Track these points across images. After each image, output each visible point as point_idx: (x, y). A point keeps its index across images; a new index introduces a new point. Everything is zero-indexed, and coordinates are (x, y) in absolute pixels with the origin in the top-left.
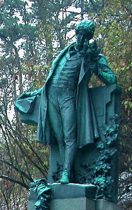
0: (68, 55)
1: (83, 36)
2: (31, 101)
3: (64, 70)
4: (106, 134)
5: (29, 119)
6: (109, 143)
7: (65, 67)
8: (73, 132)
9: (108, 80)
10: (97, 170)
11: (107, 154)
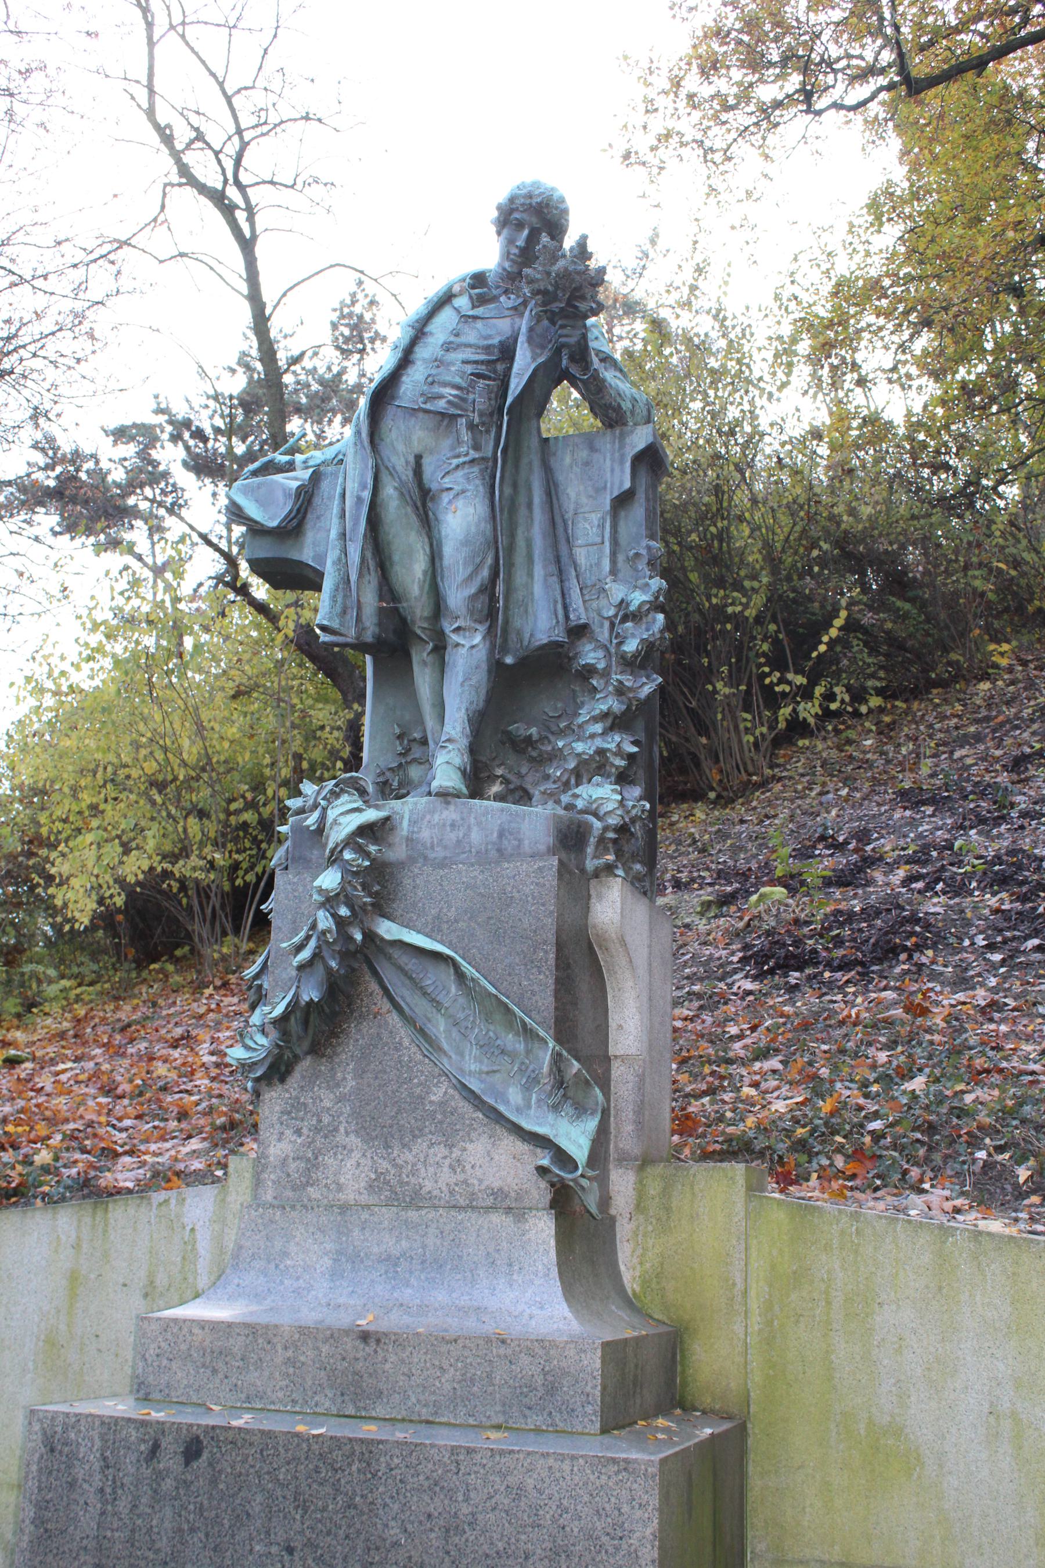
0: (462, 302)
1: (526, 232)
2: (295, 484)
3: (448, 347)
4: (616, 616)
5: (284, 555)
6: (631, 646)
7: (452, 339)
8: (482, 590)
9: (623, 404)
10: (579, 755)
11: (620, 691)
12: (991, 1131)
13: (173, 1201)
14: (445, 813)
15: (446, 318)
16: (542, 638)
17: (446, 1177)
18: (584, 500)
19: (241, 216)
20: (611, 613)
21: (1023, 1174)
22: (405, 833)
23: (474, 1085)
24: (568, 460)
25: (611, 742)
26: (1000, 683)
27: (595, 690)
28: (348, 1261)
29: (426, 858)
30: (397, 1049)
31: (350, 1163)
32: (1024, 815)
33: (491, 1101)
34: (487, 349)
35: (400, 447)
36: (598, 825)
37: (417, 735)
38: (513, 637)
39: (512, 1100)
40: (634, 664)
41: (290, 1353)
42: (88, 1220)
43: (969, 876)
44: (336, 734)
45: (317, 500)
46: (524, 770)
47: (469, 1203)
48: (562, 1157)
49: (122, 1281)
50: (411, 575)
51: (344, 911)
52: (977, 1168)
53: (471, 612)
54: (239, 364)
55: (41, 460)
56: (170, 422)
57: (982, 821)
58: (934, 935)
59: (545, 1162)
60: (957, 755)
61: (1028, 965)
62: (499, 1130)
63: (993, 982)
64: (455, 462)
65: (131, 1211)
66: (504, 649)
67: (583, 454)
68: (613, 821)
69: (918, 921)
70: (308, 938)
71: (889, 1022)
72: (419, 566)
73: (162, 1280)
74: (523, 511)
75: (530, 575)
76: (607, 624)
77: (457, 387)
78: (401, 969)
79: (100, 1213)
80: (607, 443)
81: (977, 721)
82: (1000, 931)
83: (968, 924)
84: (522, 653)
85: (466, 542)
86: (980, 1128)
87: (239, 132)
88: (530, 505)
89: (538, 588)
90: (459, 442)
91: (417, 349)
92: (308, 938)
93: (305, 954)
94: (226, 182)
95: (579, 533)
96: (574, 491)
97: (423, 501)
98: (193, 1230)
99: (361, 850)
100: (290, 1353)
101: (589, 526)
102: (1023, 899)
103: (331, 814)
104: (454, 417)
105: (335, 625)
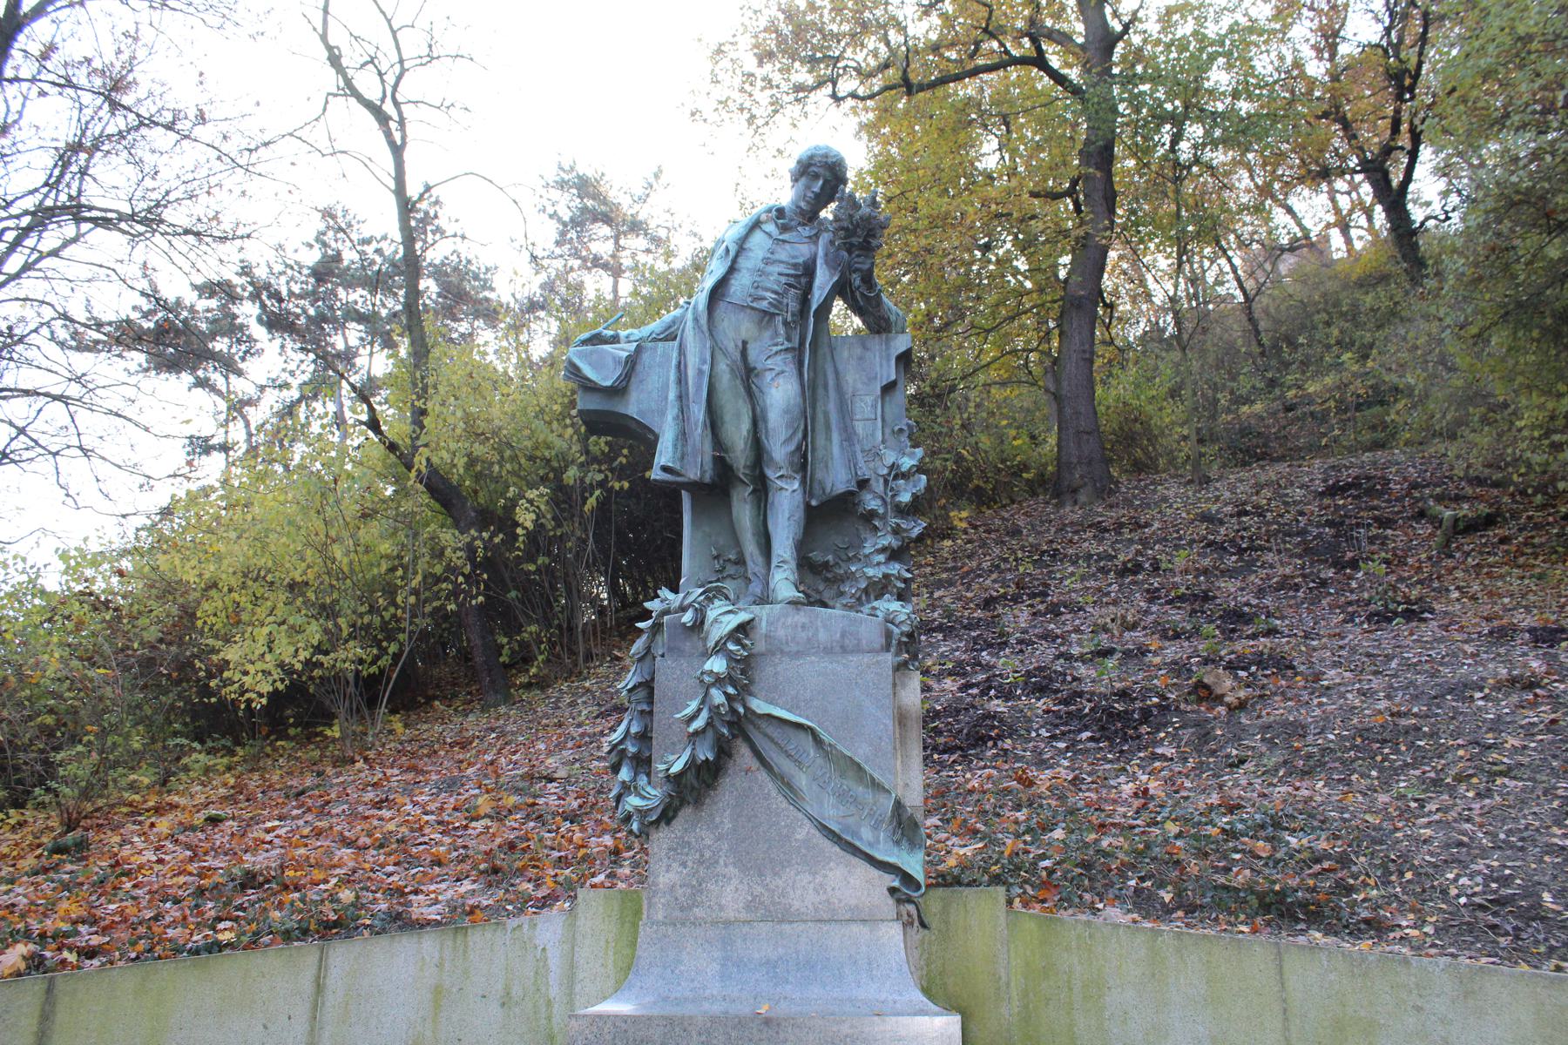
0: (770, 228)
1: (821, 182)
3: (767, 261)
6: (905, 498)
8: (799, 448)
11: (896, 531)
12: (1133, 867)
13: (526, 926)
14: (797, 618)
15: (758, 238)
16: (841, 488)
17: (811, 897)
18: (860, 386)
19: (393, 125)
20: (885, 471)
21: (1167, 896)
22: (764, 631)
24: (846, 354)
25: (895, 568)
27: (876, 529)
29: (782, 652)
30: (766, 799)
31: (729, 889)
32: (1020, 642)
33: (849, 838)
34: (795, 266)
35: (731, 334)
36: (896, 631)
37: (732, 557)
38: (816, 486)
39: (866, 837)
40: (902, 511)
41: (703, 1038)
42: (450, 943)
43: (1015, 685)
44: (459, 554)
45: (639, 368)
46: (821, 588)
47: (829, 917)
48: (907, 878)
49: (481, 993)
50: (738, 433)
51: (731, 690)
52: (1130, 892)
53: (791, 464)
54: (317, 240)
55: (146, 305)
56: (252, 283)
57: (990, 646)
59: (896, 884)
60: (936, 595)
62: (856, 861)
64: (775, 349)
65: (488, 935)
66: (811, 495)
67: (858, 351)
68: (906, 628)
69: (994, 717)
70: (699, 710)
72: (746, 425)
73: (516, 991)
74: (820, 391)
75: (829, 439)
76: (881, 481)
77: (776, 293)
78: (766, 735)
79: (460, 938)
80: (876, 343)
81: (947, 570)
82: (1056, 726)
83: (1030, 721)
84: (824, 498)
85: (787, 411)
86: (1123, 864)
87: (401, 61)
88: (826, 386)
89: (836, 450)
90: (776, 334)
91: (740, 260)
92: (699, 710)
93: (699, 724)
94: (384, 96)
95: (858, 410)
96: (851, 378)
97: (748, 375)
98: (544, 949)
99: (738, 642)
100: (703, 1038)
101: (866, 405)
102: (1066, 702)
103: (711, 614)
104: (773, 315)
105: (677, 467)
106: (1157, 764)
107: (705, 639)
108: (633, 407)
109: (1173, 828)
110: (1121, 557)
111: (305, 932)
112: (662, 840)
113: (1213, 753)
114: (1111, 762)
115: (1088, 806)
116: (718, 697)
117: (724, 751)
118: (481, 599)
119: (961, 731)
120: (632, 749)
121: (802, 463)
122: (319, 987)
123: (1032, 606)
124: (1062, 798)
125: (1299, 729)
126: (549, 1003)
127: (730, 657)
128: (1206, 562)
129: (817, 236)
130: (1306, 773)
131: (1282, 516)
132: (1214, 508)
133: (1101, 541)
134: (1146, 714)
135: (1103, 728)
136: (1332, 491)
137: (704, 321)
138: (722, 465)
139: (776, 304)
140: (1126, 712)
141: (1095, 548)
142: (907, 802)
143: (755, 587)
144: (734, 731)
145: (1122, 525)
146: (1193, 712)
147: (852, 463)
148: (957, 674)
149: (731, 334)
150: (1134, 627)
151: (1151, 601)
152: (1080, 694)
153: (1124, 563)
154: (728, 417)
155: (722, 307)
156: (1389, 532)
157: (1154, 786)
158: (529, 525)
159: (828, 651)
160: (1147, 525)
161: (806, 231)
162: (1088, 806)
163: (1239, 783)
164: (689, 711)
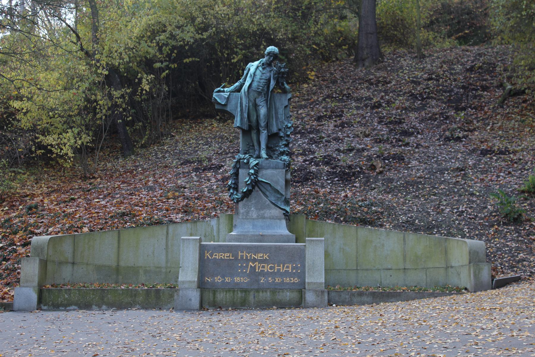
0: (260, 68)
3: (261, 79)
11: (287, 140)
12: (336, 213)
15: (258, 72)
21: (342, 219)
23: (274, 202)
25: (286, 149)
26: (310, 85)
27: (282, 140)
28: (254, 226)
32: (326, 141)
34: (266, 80)
39: (279, 204)
43: (319, 161)
48: (287, 212)
50: (254, 118)
57: (316, 142)
58: (316, 176)
60: (299, 112)
61: (336, 184)
63: (329, 187)
69: (311, 173)
71: (312, 194)
72: (255, 118)
73: (207, 234)
75: (273, 120)
80: (284, 96)
81: (305, 100)
82: (329, 176)
85: (264, 115)
89: (274, 123)
93: (248, 182)
96: (278, 104)
97: (256, 106)
101: (281, 111)
102: (333, 168)
103: (251, 161)
106: (353, 188)
107: (249, 166)
108: (228, 109)
109: (348, 205)
110: (375, 100)
111: (152, 224)
112: (241, 204)
113: (368, 186)
114: (341, 187)
115: (331, 199)
116: (252, 177)
117: (253, 187)
118: (130, 118)
119: (302, 177)
120: (233, 186)
121: (267, 126)
122: (167, 233)
123: (336, 121)
124: (325, 197)
125: (391, 181)
126: (214, 236)
127: (255, 170)
128: (407, 104)
129: (270, 71)
130: (389, 193)
131: (446, 81)
132: (420, 74)
133: (368, 88)
134: (354, 174)
135: (341, 178)
136: (471, 70)
137: (247, 94)
138: (250, 127)
139: (262, 90)
140: (349, 173)
141: (365, 93)
142: (287, 197)
143: (257, 153)
144: (256, 184)
145: (379, 82)
146: (368, 173)
147: (277, 125)
148: (303, 155)
149: (252, 97)
150: (367, 136)
151: (379, 123)
152: (338, 166)
153: (375, 103)
154: (251, 116)
155: (250, 90)
156: (485, 93)
157: (349, 194)
158: (148, 90)
159: (273, 168)
160: (390, 82)
161: (268, 69)
162: (331, 199)
163: (372, 195)
164: (247, 180)
